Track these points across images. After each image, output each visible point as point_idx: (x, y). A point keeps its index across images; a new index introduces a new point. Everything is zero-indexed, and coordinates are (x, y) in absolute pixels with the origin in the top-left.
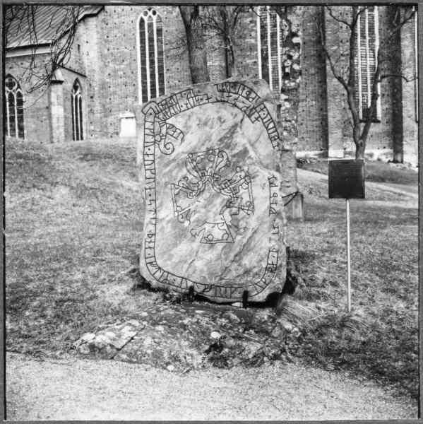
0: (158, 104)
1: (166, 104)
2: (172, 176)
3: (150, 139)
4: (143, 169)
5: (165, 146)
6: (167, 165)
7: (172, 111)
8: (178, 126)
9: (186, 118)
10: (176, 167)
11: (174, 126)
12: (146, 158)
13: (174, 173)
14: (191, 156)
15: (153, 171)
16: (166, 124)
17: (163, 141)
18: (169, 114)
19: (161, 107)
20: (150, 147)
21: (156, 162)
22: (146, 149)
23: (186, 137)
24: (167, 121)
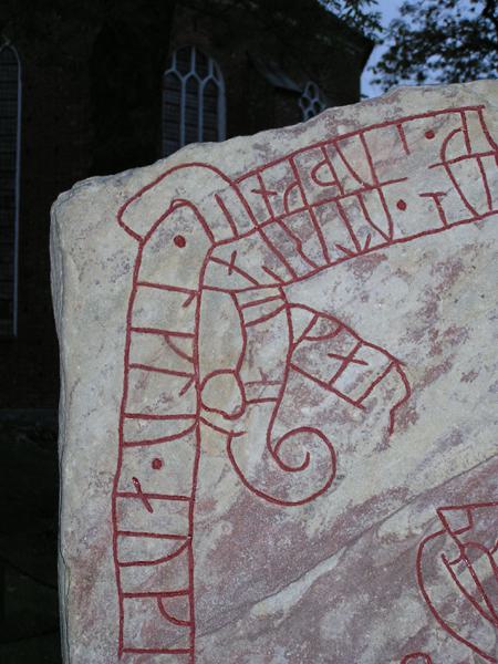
0: (234, 184)
1: (296, 182)
2: (314, 640)
3: (165, 393)
4: (105, 585)
5: (272, 449)
6: (282, 575)
7: (335, 232)
8: (369, 321)
9: (426, 278)
10: (349, 590)
11: (342, 327)
12: (136, 516)
13: (334, 625)
14: (456, 519)
15: (177, 606)
16: (288, 306)
17: (258, 416)
18: (311, 247)
19: (254, 200)
20: (162, 450)
21: (204, 545)
22: (136, 462)
23: (422, 399)
24: (298, 293)
